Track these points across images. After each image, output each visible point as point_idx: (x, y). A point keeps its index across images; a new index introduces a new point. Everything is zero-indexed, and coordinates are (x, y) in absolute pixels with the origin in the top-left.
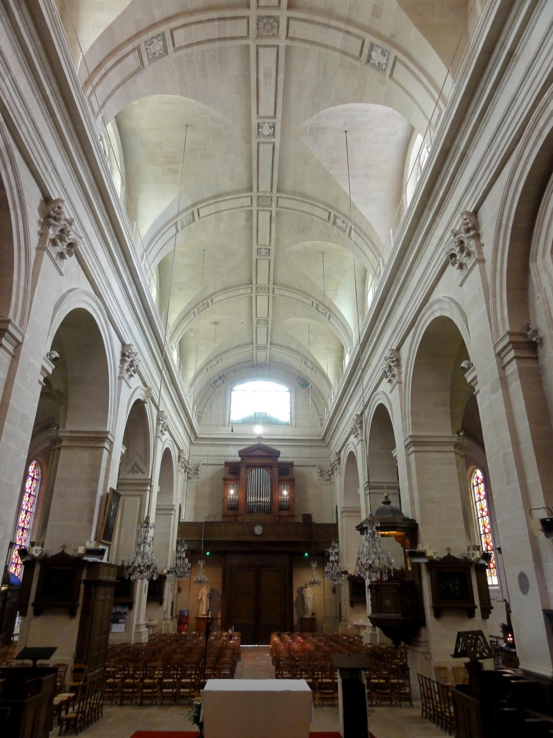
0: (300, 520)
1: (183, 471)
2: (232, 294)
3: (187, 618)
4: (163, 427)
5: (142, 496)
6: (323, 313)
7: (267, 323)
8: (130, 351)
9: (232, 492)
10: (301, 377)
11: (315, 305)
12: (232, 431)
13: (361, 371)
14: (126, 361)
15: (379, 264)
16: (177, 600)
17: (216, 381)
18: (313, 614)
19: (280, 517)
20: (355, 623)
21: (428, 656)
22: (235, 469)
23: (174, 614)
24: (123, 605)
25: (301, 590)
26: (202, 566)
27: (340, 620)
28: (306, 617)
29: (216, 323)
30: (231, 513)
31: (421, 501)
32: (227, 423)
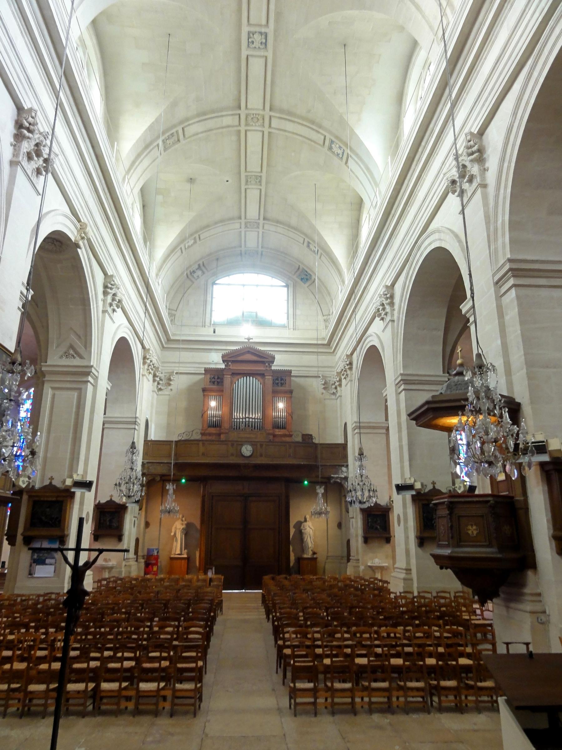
0: (299, 439)
1: (151, 377)
2: (211, 124)
3: (157, 558)
4: (113, 300)
5: (80, 389)
6: (338, 155)
7: (260, 182)
8: (30, 119)
9: (213, 404)
10: (301, 268)
11: (327, 143)
12: (214, 332)
13: (449, 105)
14: (24, 137)
15: (376, 195)
16: (144, 536)
17: (194, 272)
18: (314, 553)
19: (275, 436)
20: (369, 564)
21: (543, 618)
22: (218, 378)
23: (140, 553)
24: (51, 539)
25: (299, 525)
26: (171, 491)
27: (349, 560)
28: (305, 556)
29: (191, 180)
30: (213, 430)
31: (530, 364)
32: (207, 323)
